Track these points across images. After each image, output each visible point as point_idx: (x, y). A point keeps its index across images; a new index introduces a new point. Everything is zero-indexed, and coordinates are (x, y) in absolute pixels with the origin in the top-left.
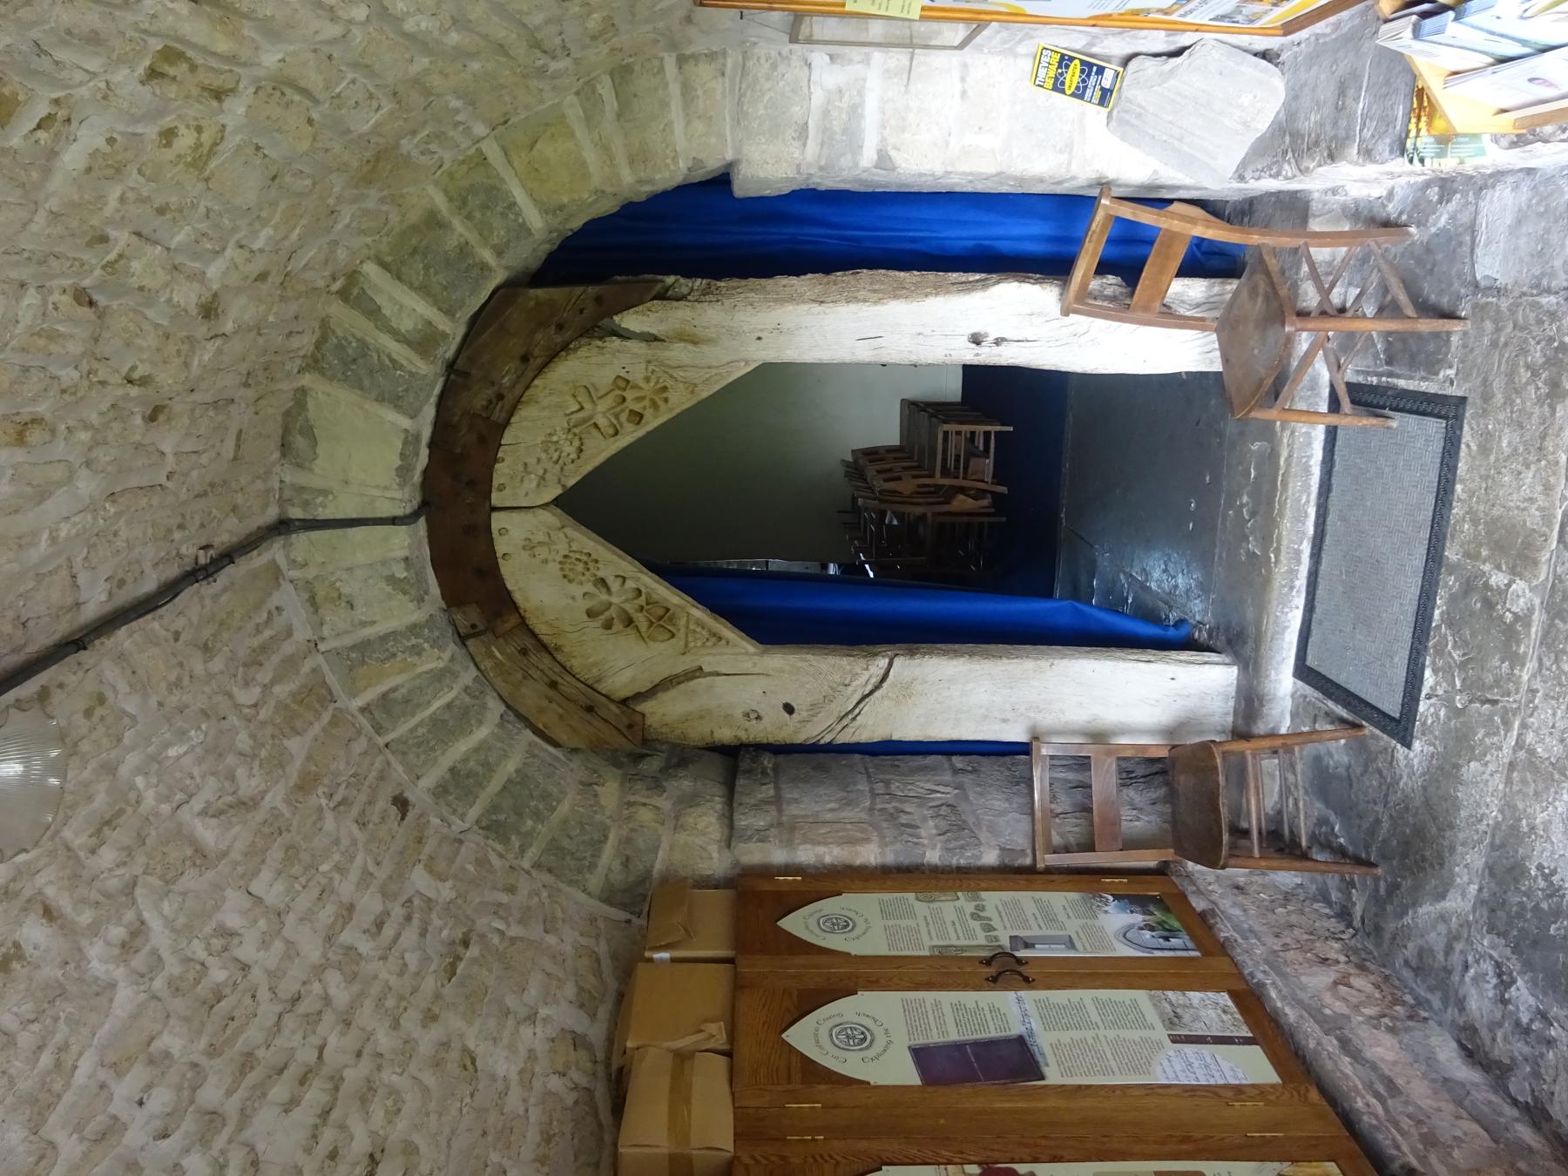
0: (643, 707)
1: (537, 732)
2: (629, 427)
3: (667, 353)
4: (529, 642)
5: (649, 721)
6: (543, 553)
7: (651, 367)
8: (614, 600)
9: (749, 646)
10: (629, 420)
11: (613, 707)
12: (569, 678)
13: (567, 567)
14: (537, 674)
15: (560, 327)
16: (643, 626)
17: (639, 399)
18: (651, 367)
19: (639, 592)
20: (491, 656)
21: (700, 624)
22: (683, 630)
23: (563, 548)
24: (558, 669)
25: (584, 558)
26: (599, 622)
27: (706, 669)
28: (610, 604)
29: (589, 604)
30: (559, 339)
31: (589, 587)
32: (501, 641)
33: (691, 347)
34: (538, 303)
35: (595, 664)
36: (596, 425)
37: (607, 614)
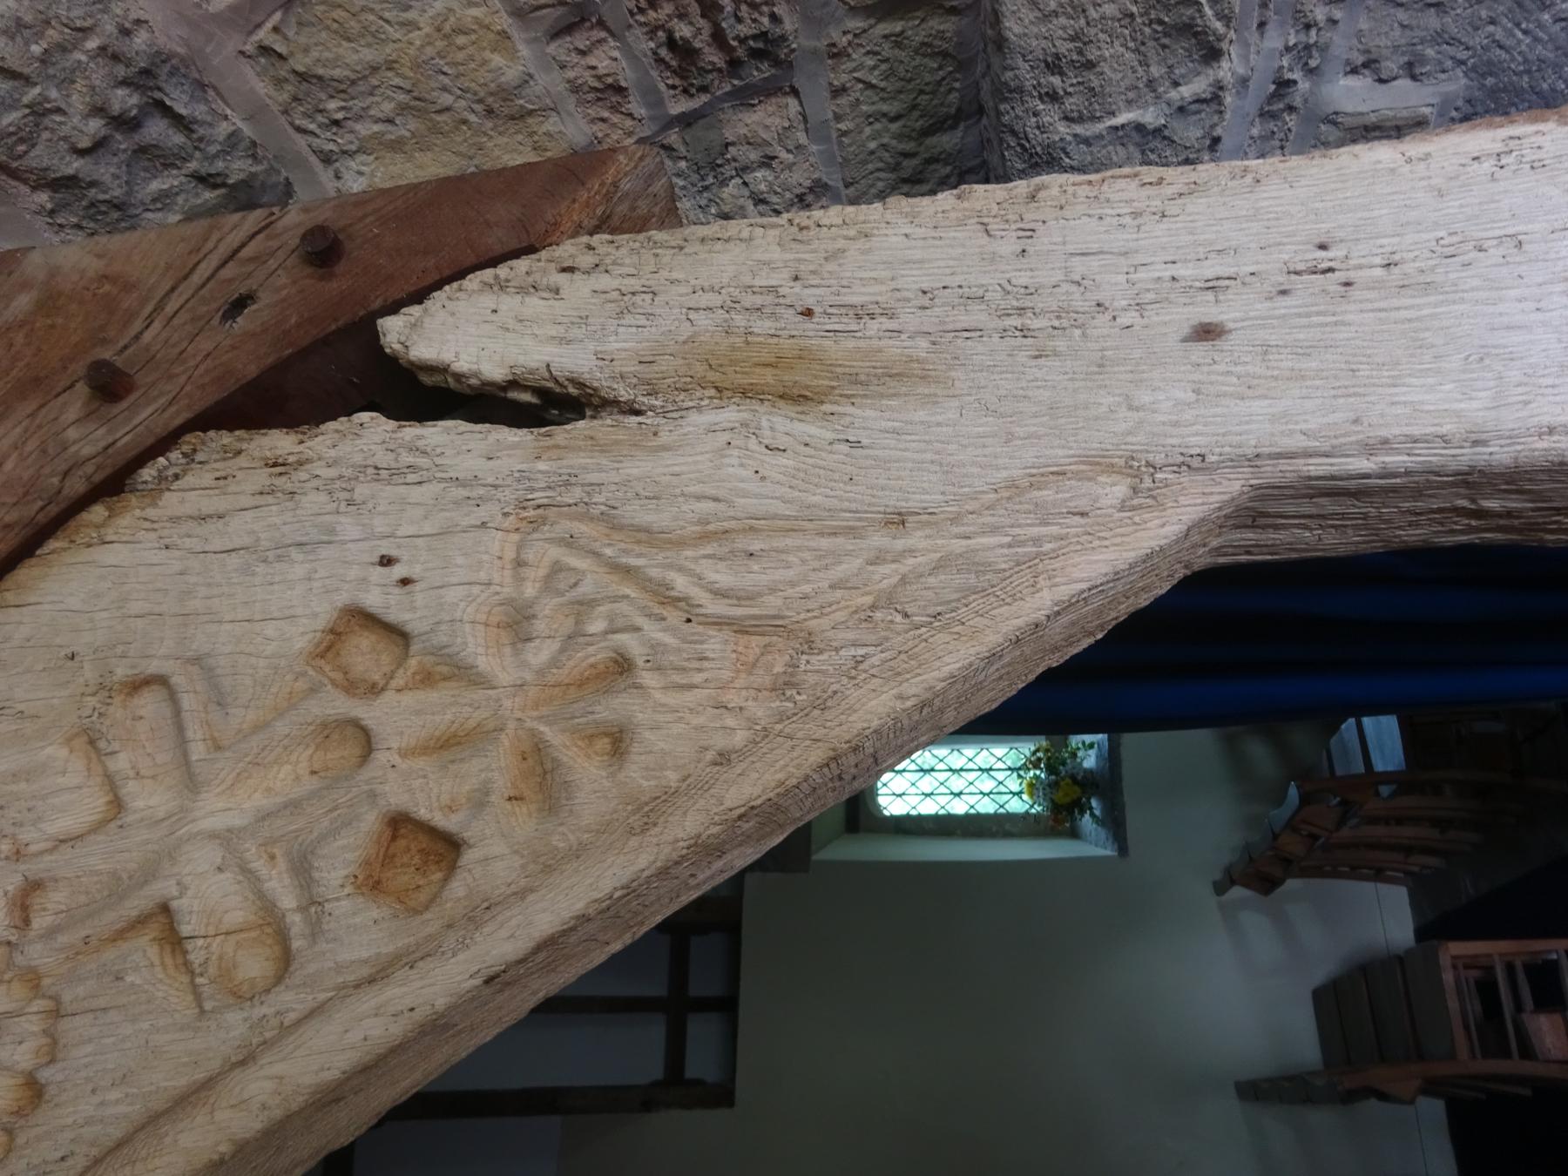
2: (361, 930)
3: (637, 467)
7: (543, 553)
10: (371, 883)
15: (109, 386)
17: (448, 745)
18: (543, 553)
30: (89, 439)
33: (779, 423)
34: (50, 302)
36: (164, 921)
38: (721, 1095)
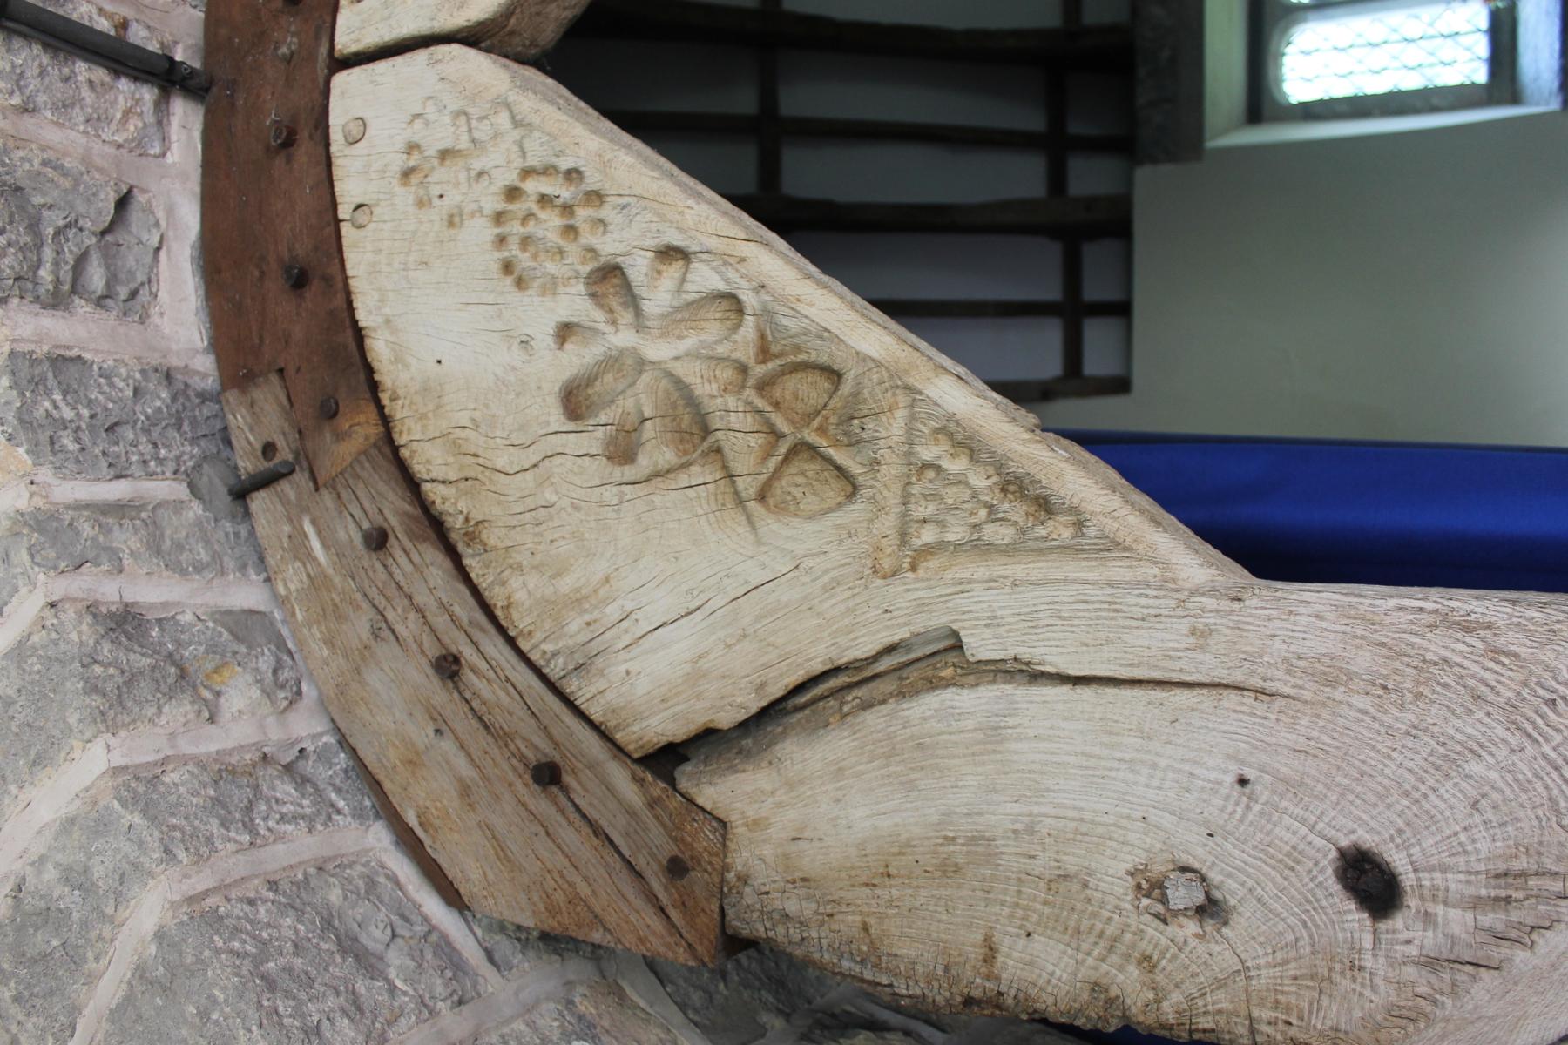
0: (723, 790)
1: (409, 842)
4: (393, 508)
5: (743, 857)
6: (450, 185)
8: (658, 350)
9: (1193, 563)
11: (620, 776)
12: (496, 648)
13: (515, 228)
14: (408, 627)
16: (743, 447)
19: (732, 301)
20: (299, 549)
21: (966, 443)
22: (892, 468)
23: (502, 165)
24: (465, 608)
25: (566, 193)
26: (593, 439)
27: (979, 646)
28: (641, 364)
29: (576, 359)
31: (574, 303)
32: (327, 497)
35: (577, 601)
37: (627, 403)
38: (1120, 385)
